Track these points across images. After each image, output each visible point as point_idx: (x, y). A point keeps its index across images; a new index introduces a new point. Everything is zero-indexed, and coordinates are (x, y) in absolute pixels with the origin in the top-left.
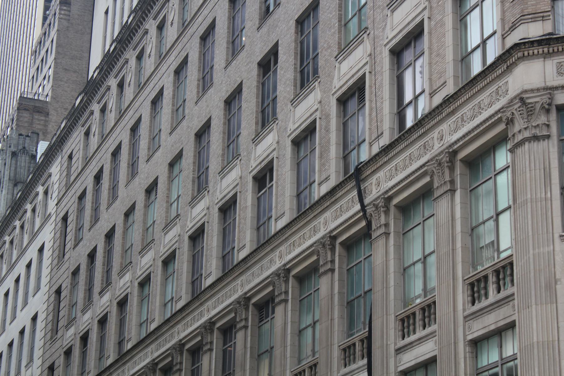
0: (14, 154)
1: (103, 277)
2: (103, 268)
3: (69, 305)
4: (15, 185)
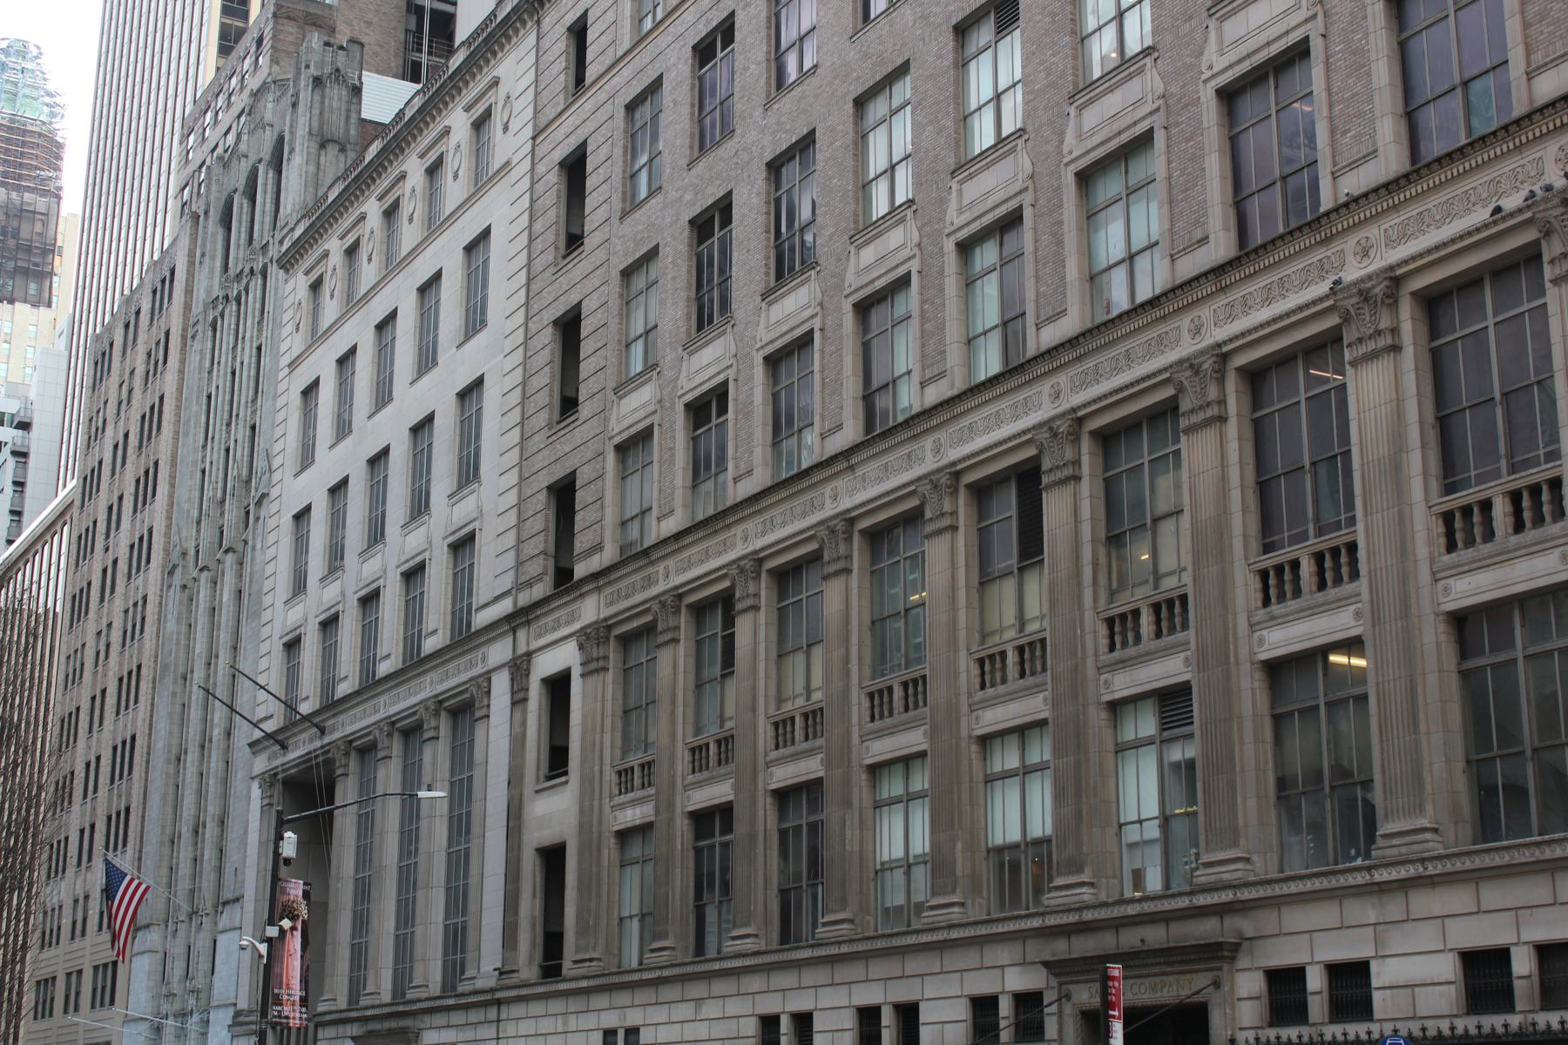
0: (318, 82)
1: (768, 258)
2: (768, 239)
3: (619, 342)
4: (323, 146)
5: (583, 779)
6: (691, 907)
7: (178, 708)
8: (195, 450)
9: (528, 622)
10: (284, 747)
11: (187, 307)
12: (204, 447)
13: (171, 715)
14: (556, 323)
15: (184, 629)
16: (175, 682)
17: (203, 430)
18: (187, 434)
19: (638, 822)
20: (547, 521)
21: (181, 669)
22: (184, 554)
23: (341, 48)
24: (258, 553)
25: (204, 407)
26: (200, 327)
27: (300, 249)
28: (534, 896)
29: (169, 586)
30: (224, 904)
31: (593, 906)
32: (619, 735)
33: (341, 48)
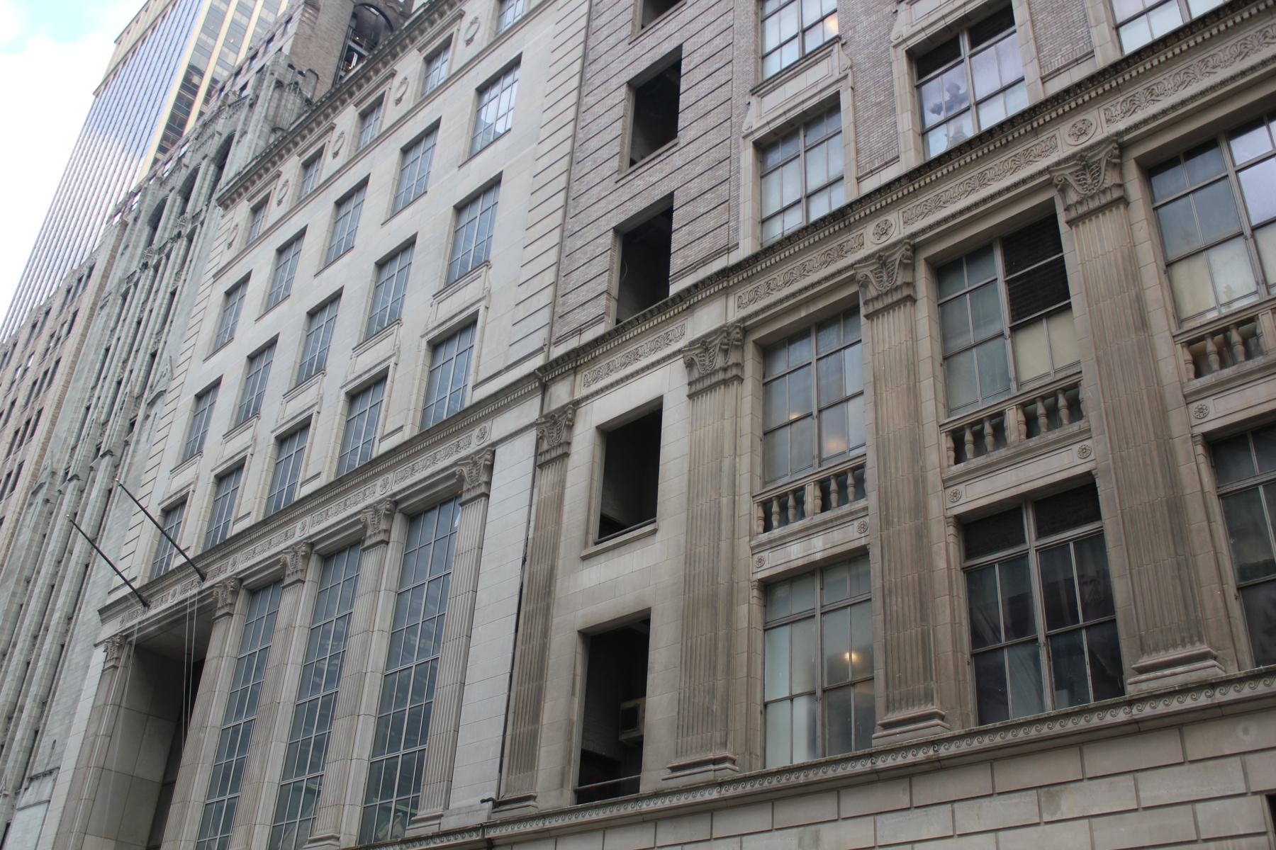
0: (279, 84)
4: (274, 130)
5: (691, 521)
6: (967, 656)
7: (15, 607)
8: (84, 390)
9: (575, 370)
10: (146, 604)
11: (101, 287)
12: (94, 388)
13: (7, 612)
14: (630, 84)
15: (38, 537)
16: (18, 583)
17: (95, 375)
18: (78, 380)
19: (818, 556)
20: (612, 260)
21: (26, 573)
22: (54, 473)
23: (301, 73)
24: (142, 446)
25: (101, 357)
26: (111, 298)
27: (245, 180)
28: (573, 694)
29: (31, 505)
30: (31, 779)
31: (720, 683)
32: (758, 460)
33: (301, 73)
